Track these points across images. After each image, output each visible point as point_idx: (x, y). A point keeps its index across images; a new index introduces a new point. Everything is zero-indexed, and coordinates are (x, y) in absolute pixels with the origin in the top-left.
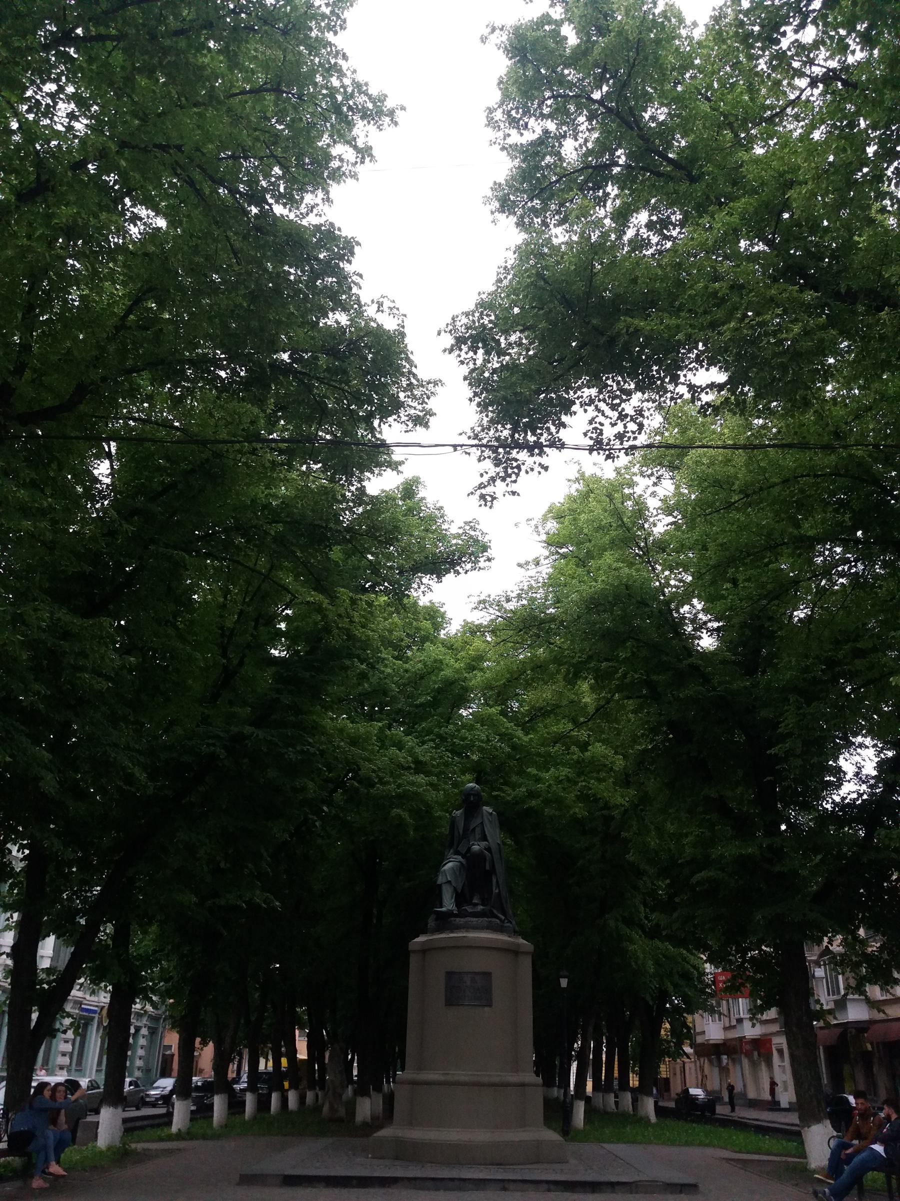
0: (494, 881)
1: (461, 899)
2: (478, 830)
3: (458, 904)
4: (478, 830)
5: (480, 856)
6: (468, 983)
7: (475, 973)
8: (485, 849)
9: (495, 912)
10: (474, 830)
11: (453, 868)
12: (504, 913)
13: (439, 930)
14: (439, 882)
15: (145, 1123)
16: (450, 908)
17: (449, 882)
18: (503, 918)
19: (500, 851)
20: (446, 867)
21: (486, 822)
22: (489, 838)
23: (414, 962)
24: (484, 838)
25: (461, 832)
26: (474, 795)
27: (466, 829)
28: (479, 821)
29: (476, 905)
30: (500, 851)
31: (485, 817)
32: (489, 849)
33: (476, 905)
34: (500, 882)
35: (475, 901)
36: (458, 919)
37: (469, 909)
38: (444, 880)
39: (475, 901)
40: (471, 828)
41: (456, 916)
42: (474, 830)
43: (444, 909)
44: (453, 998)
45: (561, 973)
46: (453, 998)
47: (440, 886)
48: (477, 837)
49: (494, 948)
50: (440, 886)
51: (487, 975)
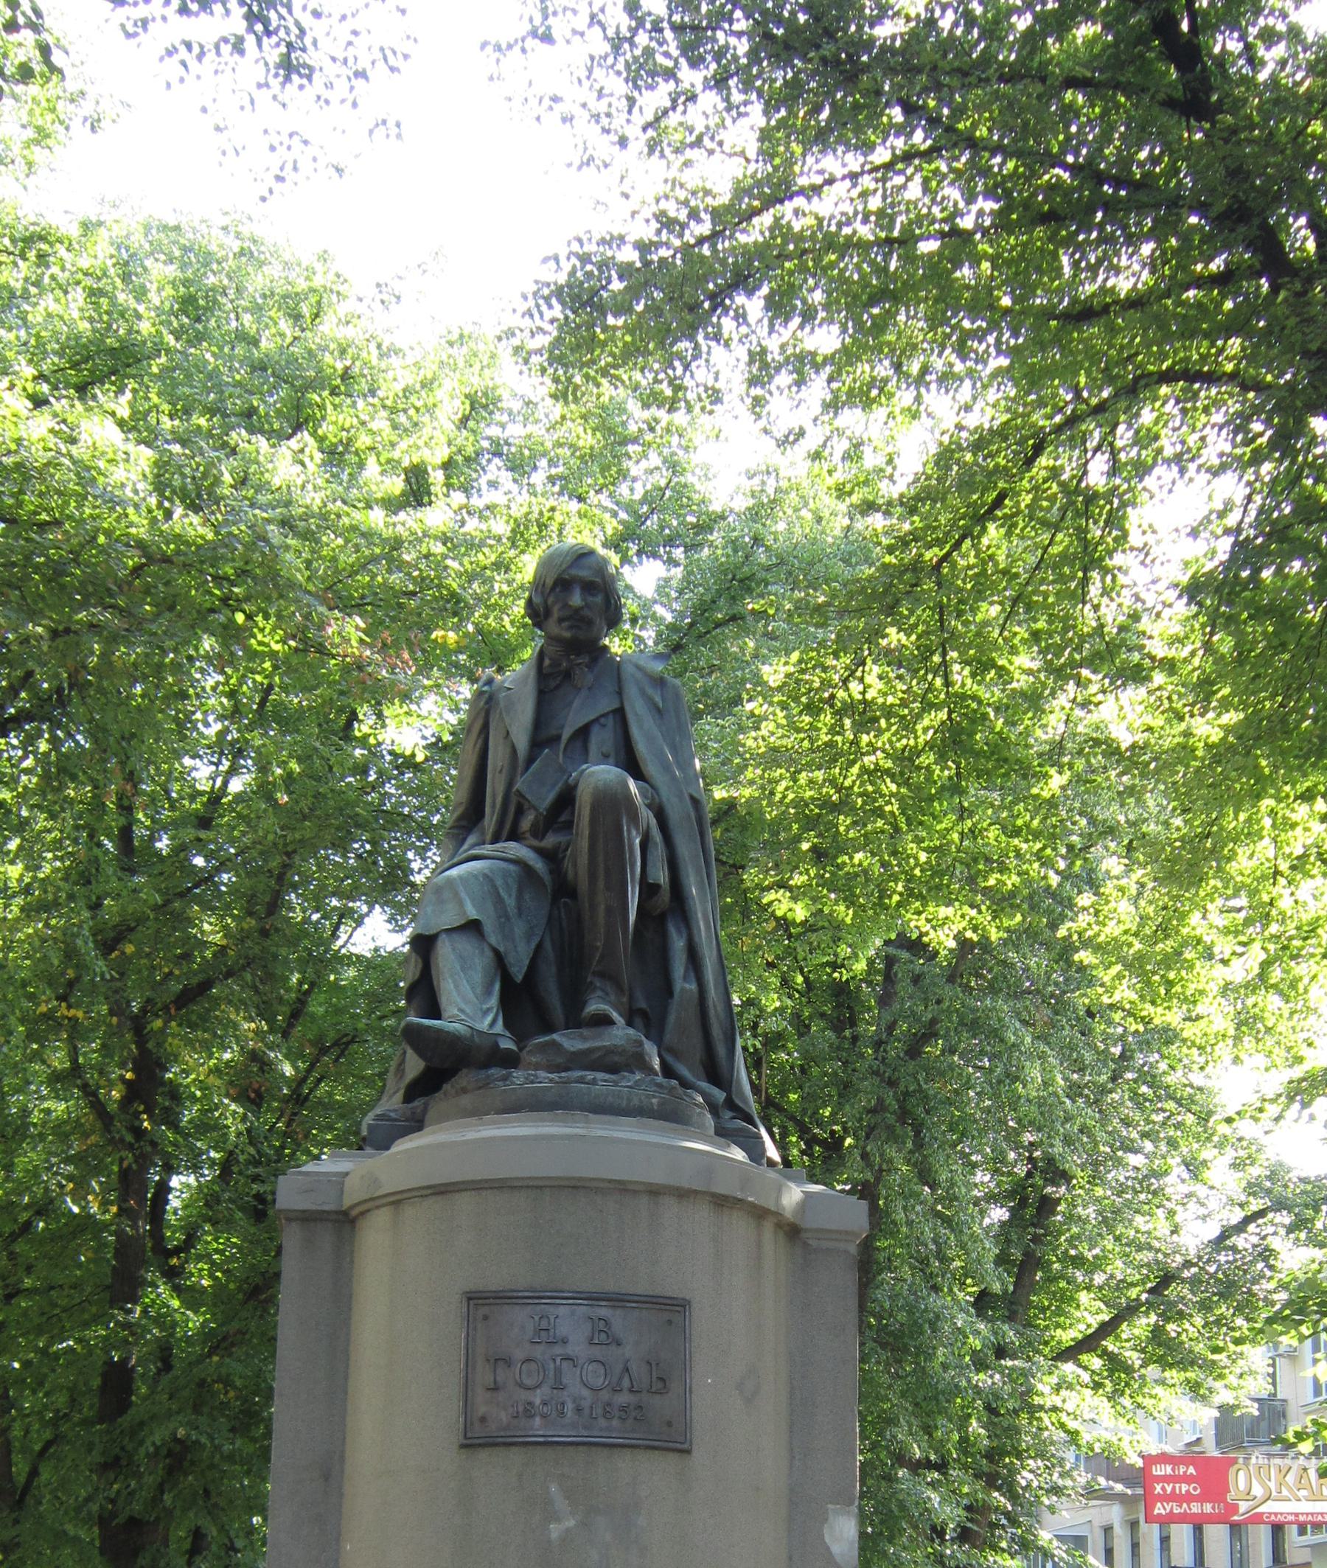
0: (678, 944)
2: (602, 739)
4: (602, 739)
6: (577, 1347)
7: (617, 1300)
11: (488, 878)
16: (484, 1025)
17: (473, 927)
22: (651, 768)
25: (522, 741)
27: (541, 739)
28: (606, 704)
29: (605, 1021)
31: (632, 692)
33: (605, 1021)
35: (595, 1006)
36: (518, 1076)
37: (570, 1041)
38: (450, 918)
39: (595, 1006)
40: (572, 720)
41: (510, 1060)
42: (583, 733)
51: (672, 1310)
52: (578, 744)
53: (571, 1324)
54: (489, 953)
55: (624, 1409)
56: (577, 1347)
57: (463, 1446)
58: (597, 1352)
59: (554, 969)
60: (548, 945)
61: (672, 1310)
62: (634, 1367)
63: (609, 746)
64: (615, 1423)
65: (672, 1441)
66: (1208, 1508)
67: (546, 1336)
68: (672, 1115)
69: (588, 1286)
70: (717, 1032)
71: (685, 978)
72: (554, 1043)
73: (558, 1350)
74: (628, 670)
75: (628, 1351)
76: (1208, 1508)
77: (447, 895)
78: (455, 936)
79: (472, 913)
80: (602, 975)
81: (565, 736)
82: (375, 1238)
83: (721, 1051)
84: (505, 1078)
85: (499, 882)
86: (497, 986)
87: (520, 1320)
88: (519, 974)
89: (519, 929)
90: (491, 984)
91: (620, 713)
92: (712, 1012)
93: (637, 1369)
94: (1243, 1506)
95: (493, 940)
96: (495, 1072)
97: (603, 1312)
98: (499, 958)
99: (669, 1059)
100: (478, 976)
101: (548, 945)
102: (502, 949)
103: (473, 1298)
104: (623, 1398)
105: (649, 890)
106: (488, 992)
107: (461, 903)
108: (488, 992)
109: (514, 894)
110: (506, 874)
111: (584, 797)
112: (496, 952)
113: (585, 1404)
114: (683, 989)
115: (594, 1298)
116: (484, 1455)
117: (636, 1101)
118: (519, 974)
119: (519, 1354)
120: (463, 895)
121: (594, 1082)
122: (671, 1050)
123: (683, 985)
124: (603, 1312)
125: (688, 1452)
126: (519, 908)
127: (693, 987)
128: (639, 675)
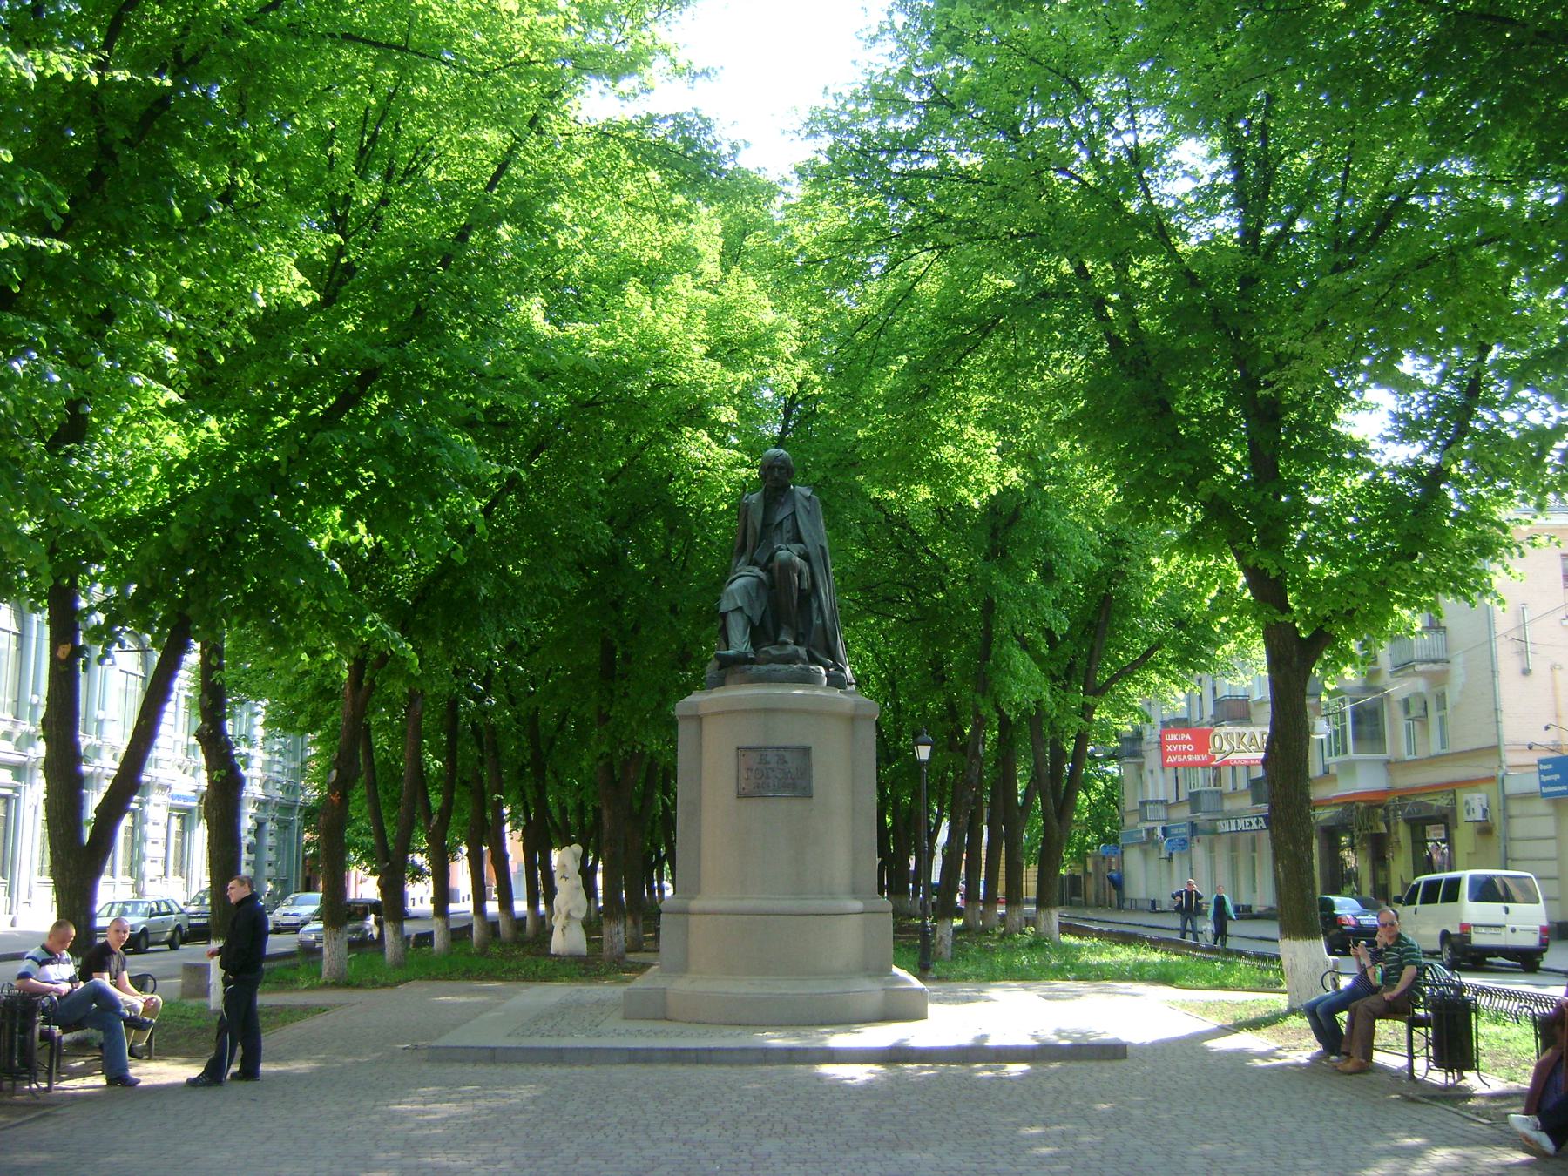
0: (815, 605)
1: (760, 634)
2: (787, 525)
3: (755, 643)
4: (787, 525)
5: (787, 566)
7: (785, 748)
9: (817, 654)
13: (720, 682)
14: (722, 610)
16: (742, 649)
17: (740, 609)
20: (734, 586)
21: (801, 512)
24: (798, 538)
25: (759, 527)
26: (780, 468)
27: (766, 524)
28: (787, 511)
29: (786, 643)
35: (783, 638)
36: (755, 667)
37: (774, 651)
38: (731, 607)
39: (783, 638)
40: (779, 518)
41: (752, 661)
42: (781, 523)
43: (731, 652)
47: (724, 616)
48: (786, 536)
49: (758, 711)
50: (724, 616)
51: (806, 751)
53: (771, 757)
57: (739, 796)
61: (806, 751)
65: (806, 793)
66: (1197, 758)
68: (807, 679)
69: (777, 744)
76: (1197, 758)
82: (709, 728)
91: (794, 514)
94: (1218, 756)
100: (741, 628)
105: (800, 590)
111: (776, 560)
115: (778, 748)
123: (817, 622)
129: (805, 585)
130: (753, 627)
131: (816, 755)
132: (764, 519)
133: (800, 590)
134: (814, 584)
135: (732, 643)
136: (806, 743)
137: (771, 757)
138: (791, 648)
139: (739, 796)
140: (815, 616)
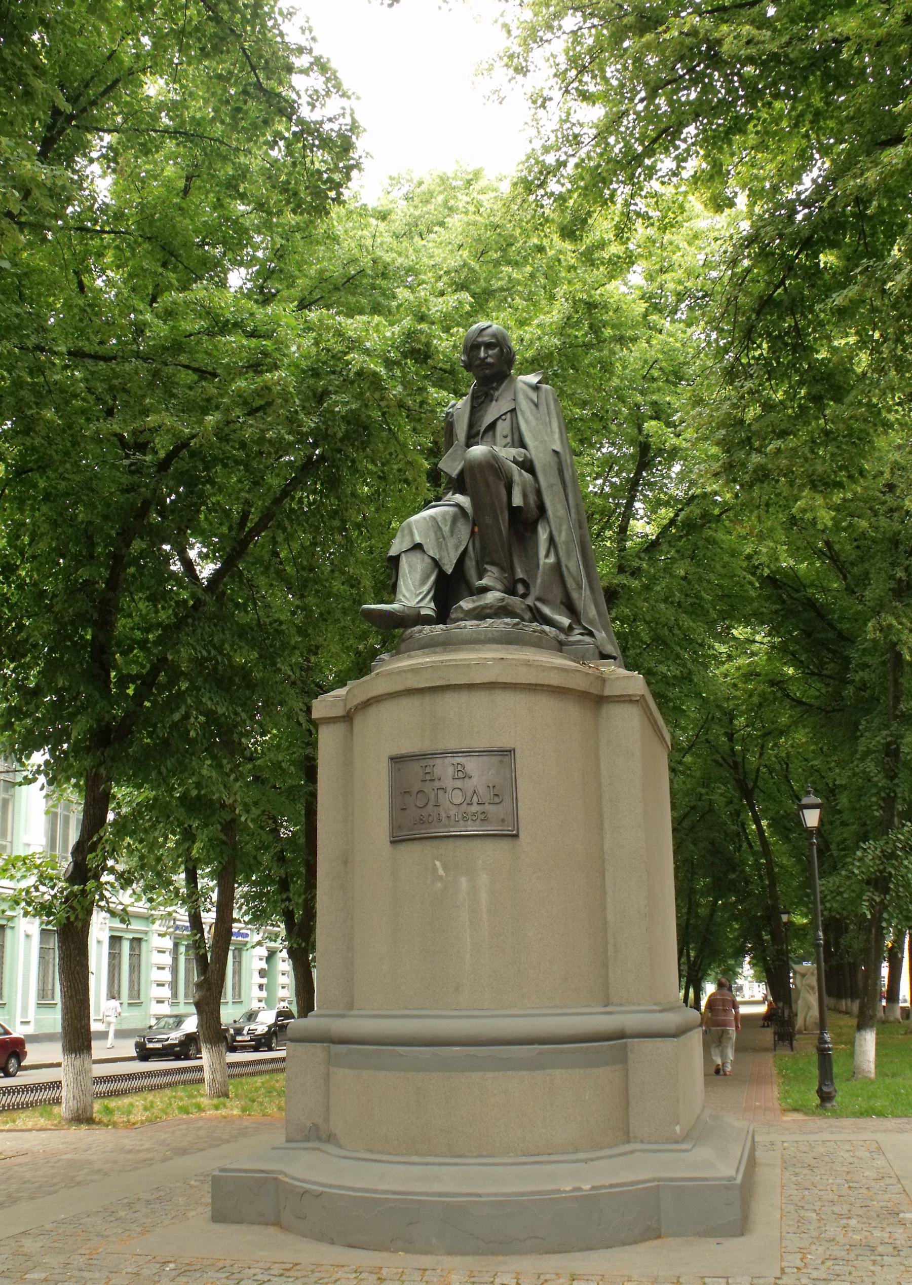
2: (503, 427)
7: (468, 753)
8: (515, 462)
9: (546, 610)
10: (492, 426)
11: (433, 518)
12: (571, 609)
14: (393, 552)
15: (146, 1082)
16: (413, 603)
17: (418, 547)
18: (566, 621)
19: (561, 471)
21: (524, 406)
22: (528, 440)
23: (328, 742)
26: (489, 346)
30: (561, 471)
31: (521, 398)
32: (528, 466)
33: (485, 590)
34: (561, 538)
35: (485, 582)
37: (466, 604)
38: (407, 545)
41: (427, 620)
42: (492, 426)
44: (415, 820)
45: (805, 801)
46: (415, 820)
50: (395, 561)
52: (491, 433)
54: (429, 561)
55: (474, 815)
56: (449, 783)
58: (459, 784)
59: (474, 563)
60: (470, 548)
62: (481, 790)
63: (507, 431)
64: (470, 822)
67: (429, 778)
69: (452, 745)
70: (570, 583)
71: (547, 556)
72: (460, 607)
73: (437, 784)
74: (520, 385)
75: (475, 780)
77: (406, 532)
78: (408, 554)
79: (418, 540)
80: (492, 563)
81: (483, 429)
83: (575, 595)
84: (421, 631)
85: (439, 519)
86: (433, 578)
87: (416, 767)
88: (449, 570)
89: (451, 543)
90: (428, 577)
91: (513, 411)
92: (565, 573)
93: (481, 790)
95: (431, 553)
96: (416, 628)
97: (459, 760)
98: (436, 563)
99: (539, 604)
100: (418, 576)
101: (470, 548)
102: (437, 557)
103: (393, 759)
104: (475, 808)
106: (423, 582)
107: (412, 534)
108: (423, 582)
109: (449, 523)
110: (444, 515)
112: (433, 559)
113: (452, 813)
114: (545, 564)
116: (403, 847)
117: (490, 635)
118: (449, 570)
119: (416, 789)
120: (415, 531)
121: (465, 627)
122: (539, 599)
123: (546, 560)
124: (459, 760)
125: (516, 836)
126: (452, 532)
127: (552, 560)
128: (525, 388)
129: (517, 501)
130: (441, 574)
131: (523, 761)
132: (471, 425)
133: (515, 512)
134: (542, 509)
135: (399, 596)
136: (504, 742)
137: (444, 769)
138: (491, 597)
139: (392, 842)
140: (542, 552)
